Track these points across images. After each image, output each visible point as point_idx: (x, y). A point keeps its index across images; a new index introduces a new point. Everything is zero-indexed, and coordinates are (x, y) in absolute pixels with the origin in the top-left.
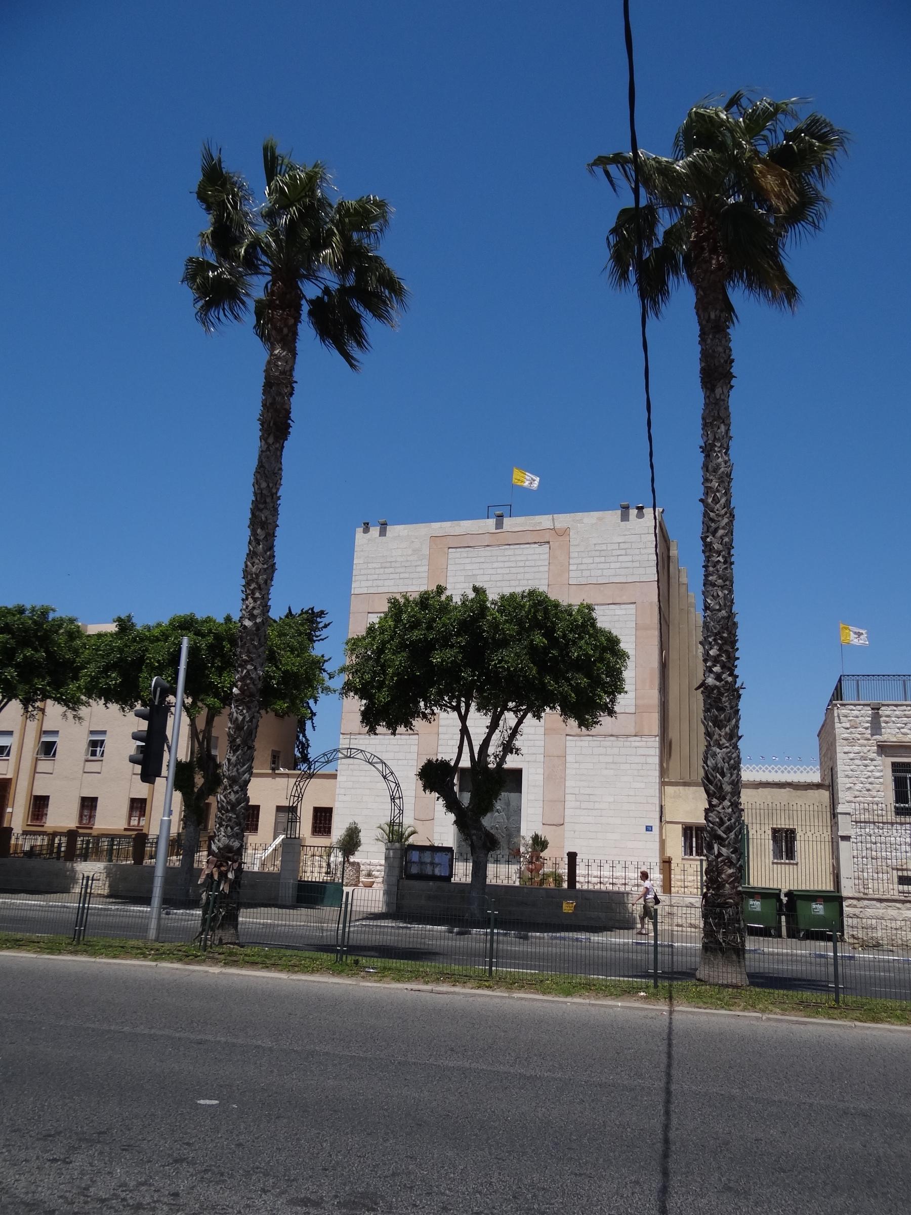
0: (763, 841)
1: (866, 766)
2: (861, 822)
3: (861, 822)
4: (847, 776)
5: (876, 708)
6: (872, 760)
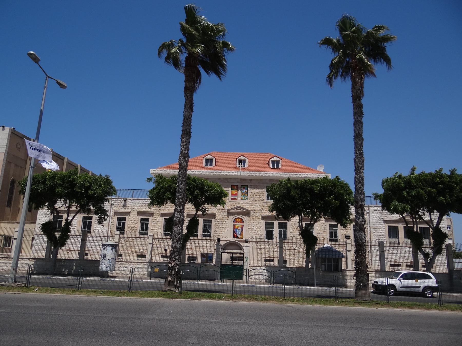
0: (28, 241)
1: (46, 216)
2: (40, 234)
3: (40, 234)
4: (39, 220)
5: (125, 200)
6: (48, 214)
